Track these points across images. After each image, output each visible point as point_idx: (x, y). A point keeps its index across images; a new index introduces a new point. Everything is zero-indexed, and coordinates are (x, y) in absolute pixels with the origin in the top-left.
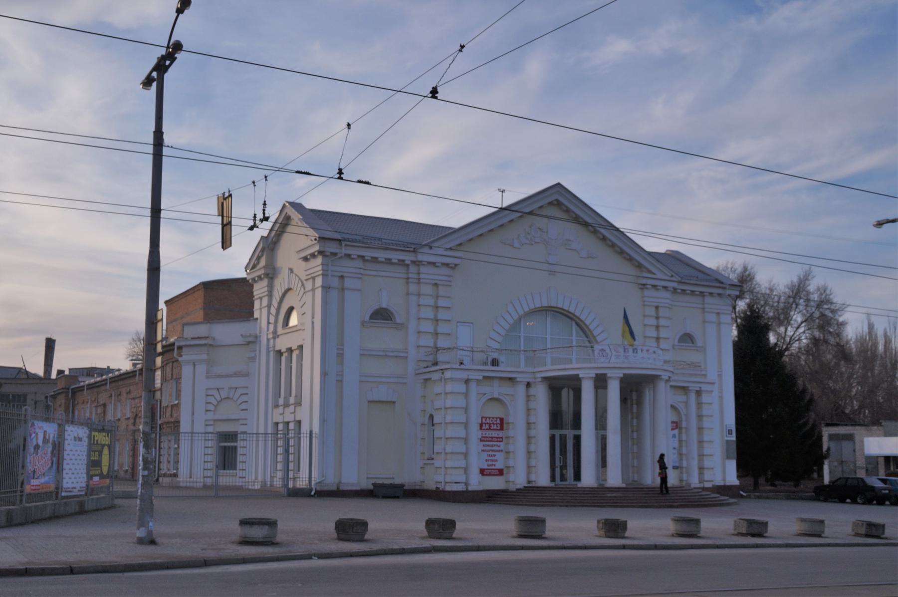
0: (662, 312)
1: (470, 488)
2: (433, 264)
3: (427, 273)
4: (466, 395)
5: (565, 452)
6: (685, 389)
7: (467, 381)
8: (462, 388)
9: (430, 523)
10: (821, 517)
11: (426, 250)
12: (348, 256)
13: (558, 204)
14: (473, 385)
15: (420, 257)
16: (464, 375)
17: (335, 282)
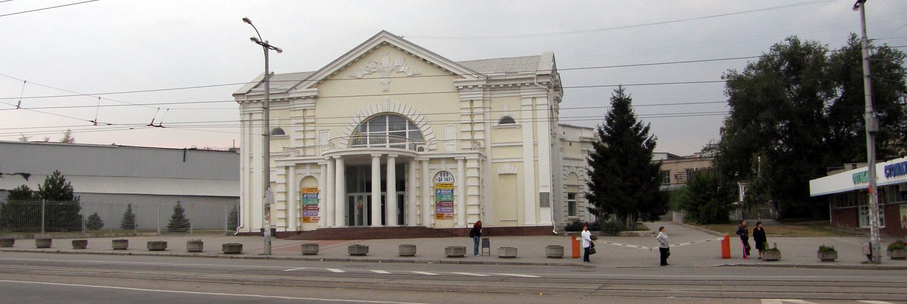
0: (476, 104)
1: (288, 230)
2: (300, 98)
3: (300, 104)
4: (286, 176)
5: (356, 209)
6: (452, 160)
7: (287, 168)
8: (283, 171)
9: (73, 242)
10: (463, 245)
11: (294, 91)
12: (251, 101)
13: (384, 45)
14: (291, 170)
15: (291, 96)
16: (283, 164)
17: (247, 117)
